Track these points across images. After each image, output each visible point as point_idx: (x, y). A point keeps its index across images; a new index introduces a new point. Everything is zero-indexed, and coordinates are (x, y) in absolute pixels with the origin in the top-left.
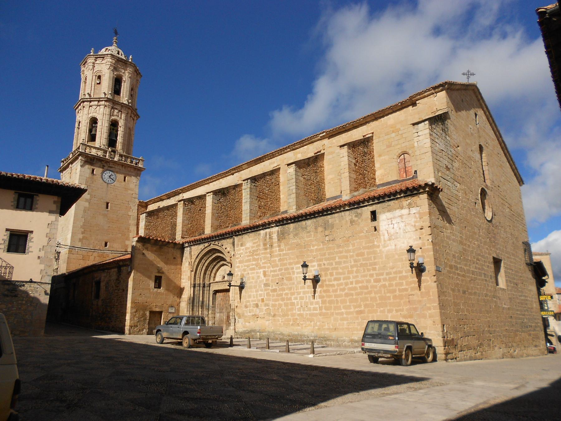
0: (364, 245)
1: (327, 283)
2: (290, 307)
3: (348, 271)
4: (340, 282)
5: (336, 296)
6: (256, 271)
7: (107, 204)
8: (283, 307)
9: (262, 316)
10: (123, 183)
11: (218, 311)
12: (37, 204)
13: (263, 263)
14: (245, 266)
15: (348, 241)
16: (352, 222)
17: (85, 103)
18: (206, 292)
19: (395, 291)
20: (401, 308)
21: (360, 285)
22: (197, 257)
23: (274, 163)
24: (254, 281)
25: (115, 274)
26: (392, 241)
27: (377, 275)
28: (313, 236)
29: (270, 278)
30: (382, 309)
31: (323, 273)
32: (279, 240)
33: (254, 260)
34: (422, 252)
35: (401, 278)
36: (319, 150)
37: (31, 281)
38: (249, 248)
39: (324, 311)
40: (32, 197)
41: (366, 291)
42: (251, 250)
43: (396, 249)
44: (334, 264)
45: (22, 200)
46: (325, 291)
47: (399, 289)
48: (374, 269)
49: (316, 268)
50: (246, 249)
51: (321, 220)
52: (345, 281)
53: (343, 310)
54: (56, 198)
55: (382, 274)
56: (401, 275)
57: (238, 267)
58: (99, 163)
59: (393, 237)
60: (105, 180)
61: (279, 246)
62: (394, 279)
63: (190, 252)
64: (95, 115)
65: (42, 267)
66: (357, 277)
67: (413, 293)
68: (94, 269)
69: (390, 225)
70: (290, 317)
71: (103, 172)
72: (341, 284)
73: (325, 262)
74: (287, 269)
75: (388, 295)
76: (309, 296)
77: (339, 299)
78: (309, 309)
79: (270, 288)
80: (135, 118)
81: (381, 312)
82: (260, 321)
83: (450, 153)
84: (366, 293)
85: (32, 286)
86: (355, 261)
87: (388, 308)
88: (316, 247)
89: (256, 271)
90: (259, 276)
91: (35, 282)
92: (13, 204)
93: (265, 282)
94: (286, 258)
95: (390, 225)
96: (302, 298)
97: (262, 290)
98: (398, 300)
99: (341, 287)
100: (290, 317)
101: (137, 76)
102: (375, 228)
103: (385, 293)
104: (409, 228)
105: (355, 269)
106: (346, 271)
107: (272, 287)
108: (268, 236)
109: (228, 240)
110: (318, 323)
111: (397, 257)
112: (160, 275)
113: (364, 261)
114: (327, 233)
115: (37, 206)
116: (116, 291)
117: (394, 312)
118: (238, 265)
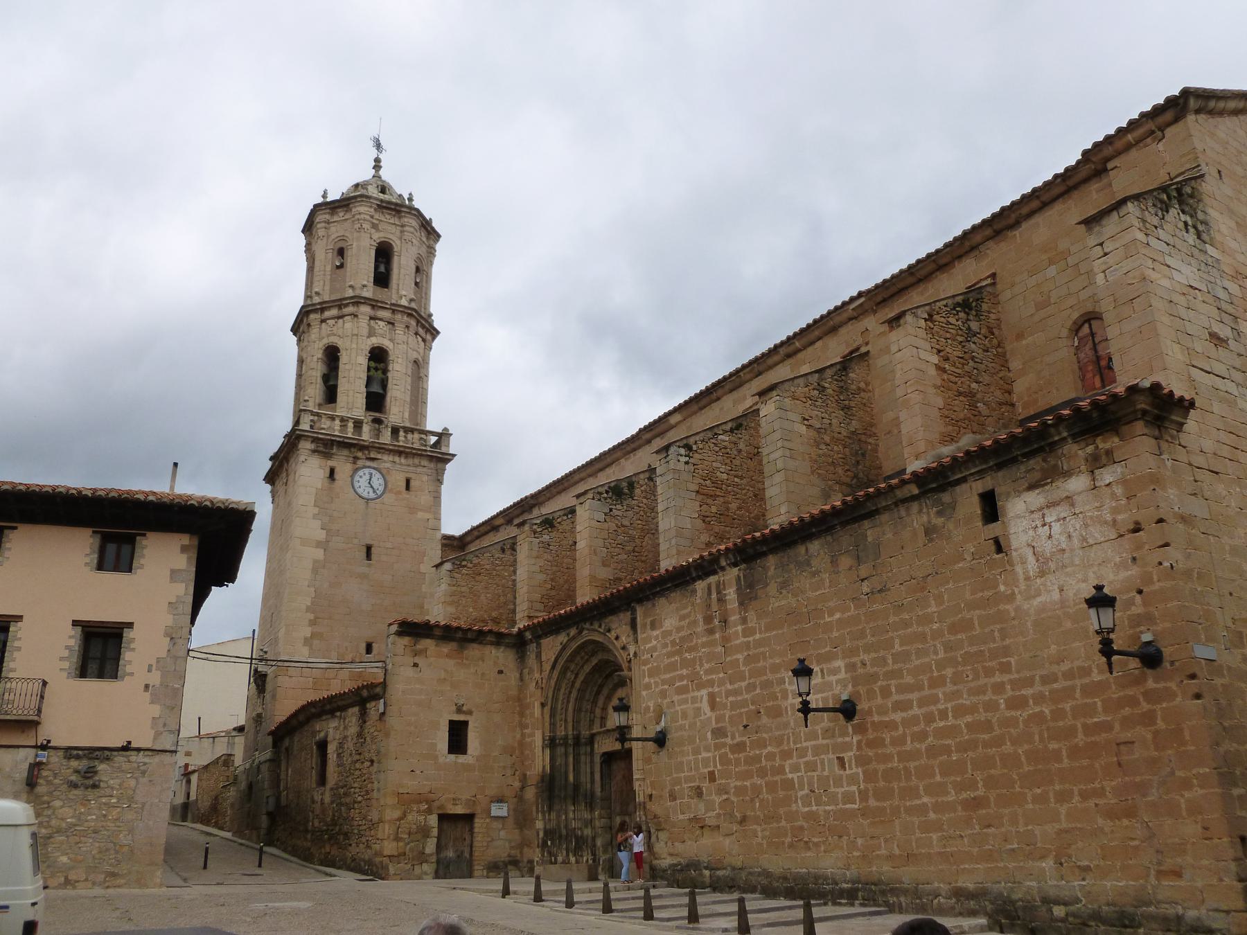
0: (968, 596)
1: (876, 718)
2: (781, 794)
3: (931, 678)
4: (911, 713)
5: (904, 757)
6: (689, 696)
7: (369, 549)
8: (765, 795)
9: (713, 822)
10: (405, 495)
11: (618, 810)
12: (143, 556)
13: (707, 672)
14: (664, 682)
15: (923, 589)
16: (929, 531)
17: (312, 316)
18: (583, 758)
19: (1070, 732)
20: (1097, 785)
21: (969, 719)
22: (553, 667)
23: (745, 398)
24: (687, 723)
25: (354, 720)
26: (1051, 577)
27: (1015, 684)
28: (827, 584)
29: (728, 714)
30: (1039, 791)
31: (862, 690)
32: (741, 604)
33: (685, 663)
34: (1145, 604)
35: (1088, 691)
36: (855, 346)
37: (126, 748)
38: (669, 633)
39: (872, 803)
40: (131, 541)
41: (986, 736)
42: (676, 637)
43: (1063, 603)
44: (890, 661)
45: (111, 548)
46: (871, 744)
47: (1085, 726)
48: (1005, 668)
49: (842, 675)
50: (667, 634)
51: (845, 538)
52: (923, 710)
53: (925, 800)
54: (185, 539)
55: (1030, 682)
56: (1086, 680)
57: (648, 686)
58: (345, 452)
59: (1052, 565)
60: (360, 491)
61: (744, 621)
62: (1068, 693)
63: (539, 655)
64: (334, 340)
65: (156, 710)
66: (956, 695)
67: (1128, 735)
68: (313, 710)
69: (1040, 530)
70: (783, 823)
71: (356, 470)
72: (914, 720)
73: (866, 657)
74: (767, 685)
75: (1053, 746)
76: (829, 760)
77: (912, 765)
78: (833, 799)
79: (729, 740)
80: (429, 337)
81: (1036, 799)
82: (707, 841)
83: (1222, 294)
84: (986, 745)
85: (133, 758)
86: (948, 647)
87: (1057, 787)
88: (837, 616)
89: (692, 694)
90: (699, 709)
91: (138, 750)
92: (87, 560)
93: (714, 725)
94: (763, 654)
95: (1040, 530)
96: (811, 767)
97: (707, 749)
98: (1085, 762)
99: (916, 729)
100: (783, 823)
101: (428, 238)
102: (997, 542)
103: (1042, 740)
104: (1097, 533)
105: (949, 672)
106: (925, 679)
107: (733, 738)
108: (714, 596)
109: (622, 615)
110: (860, 841)
111: (1068, 624)
112: (461, 718)
113: (971, 645)
114: (864, 571)
115: (142, 561)
116: (358, 765)
117: (1076, 798)
118: (647, 680)
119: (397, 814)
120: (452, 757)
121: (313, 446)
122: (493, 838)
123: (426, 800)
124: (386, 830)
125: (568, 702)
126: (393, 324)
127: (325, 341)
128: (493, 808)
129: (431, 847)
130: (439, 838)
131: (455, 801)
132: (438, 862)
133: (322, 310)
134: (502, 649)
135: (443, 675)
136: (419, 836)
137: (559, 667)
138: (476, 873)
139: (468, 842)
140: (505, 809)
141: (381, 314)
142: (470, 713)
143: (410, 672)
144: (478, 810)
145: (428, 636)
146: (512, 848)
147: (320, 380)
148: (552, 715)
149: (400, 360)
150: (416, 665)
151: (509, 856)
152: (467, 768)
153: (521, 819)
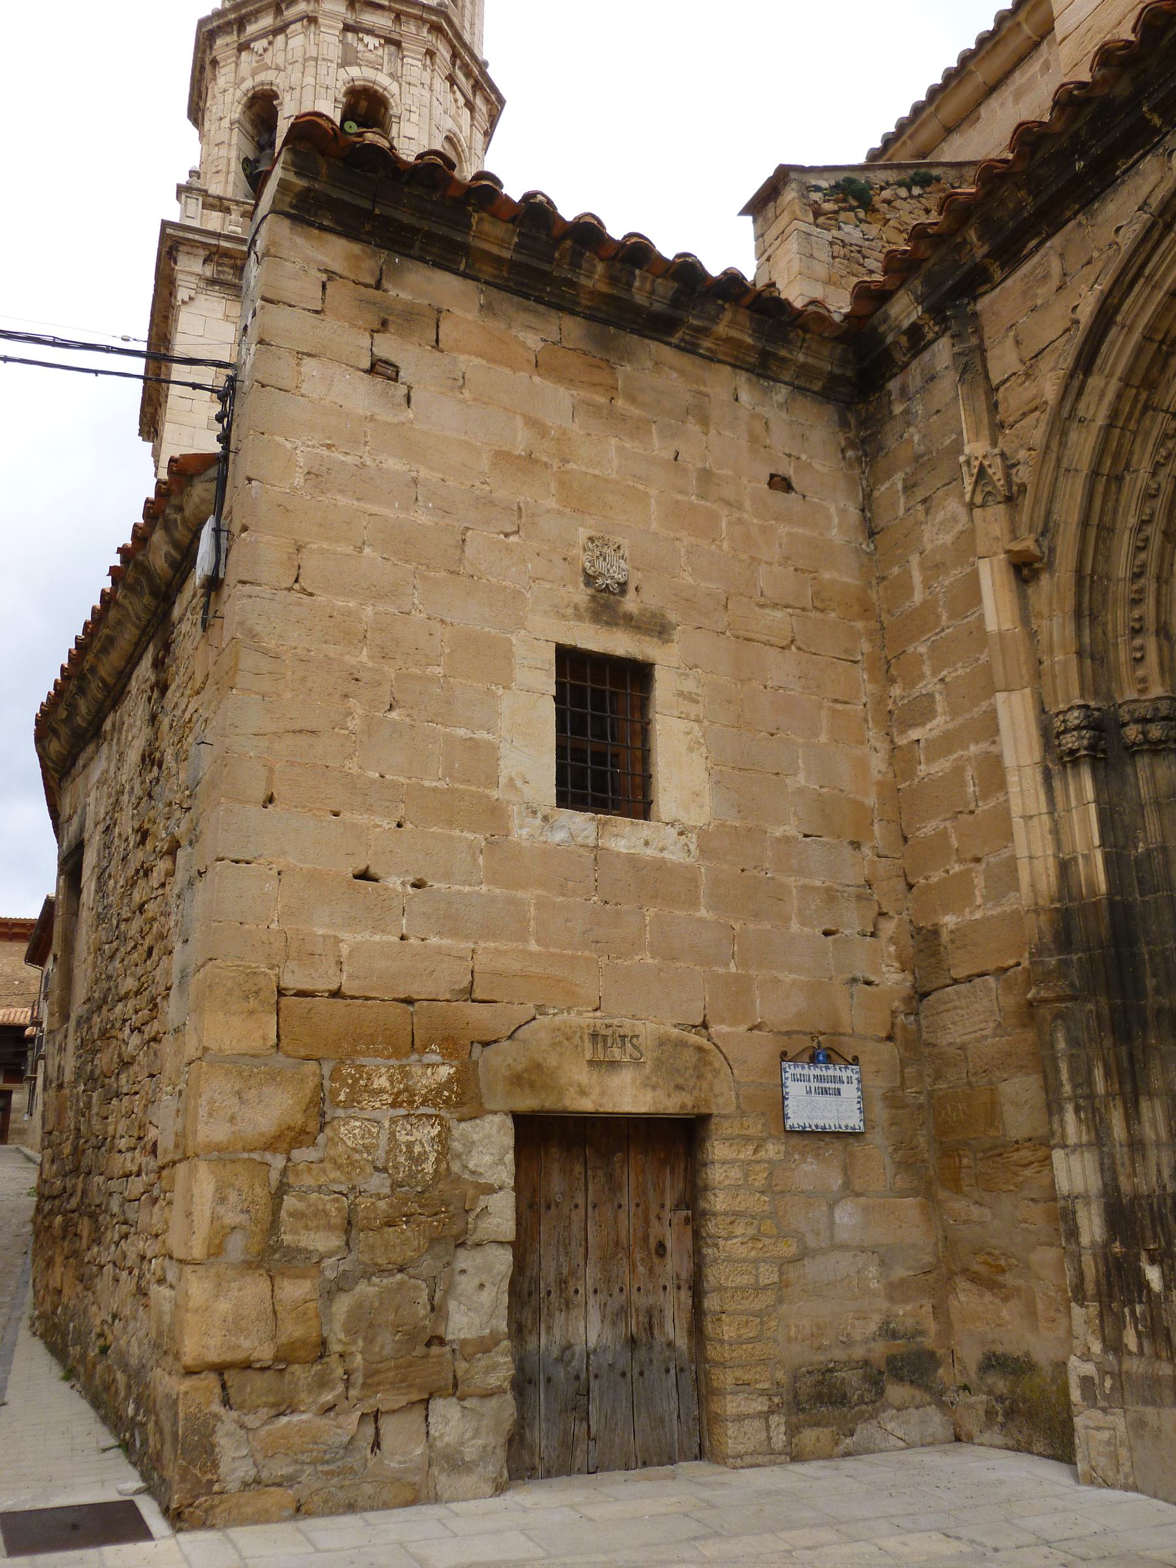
17: (220, 42)
22: (1086, 360)
119: (274, 1108)
120: (579, 824)
121: (208, 271)
122: (806, 1237)
123: (445, 1034)
124: (201, 1202)
126: (398, 44)
127: (248, 84)
128: (795, 1090)
129: (476, 1304)
130: (523, 1246)
131: (605, 1047)
132: (523, 1384)
133: (241, 23)
134: (781, 393)
135: (520, 439)
136: (406, 1240)
137: (1120, 351)
138: (736, 1438)
139: (676, 1264)
140: (850, 1091)
141: (370, 18)
142: (660, 629)
143: (360, 396)
144: (722, 1098)
145: (449, 255)
146: (896, 1291)
147: (235, 167)
148: (1087, 610)
149: (414, 117)
150: (381, 369)
151: (889, 1332)
152: (653, 880)
153: (943, 1141)
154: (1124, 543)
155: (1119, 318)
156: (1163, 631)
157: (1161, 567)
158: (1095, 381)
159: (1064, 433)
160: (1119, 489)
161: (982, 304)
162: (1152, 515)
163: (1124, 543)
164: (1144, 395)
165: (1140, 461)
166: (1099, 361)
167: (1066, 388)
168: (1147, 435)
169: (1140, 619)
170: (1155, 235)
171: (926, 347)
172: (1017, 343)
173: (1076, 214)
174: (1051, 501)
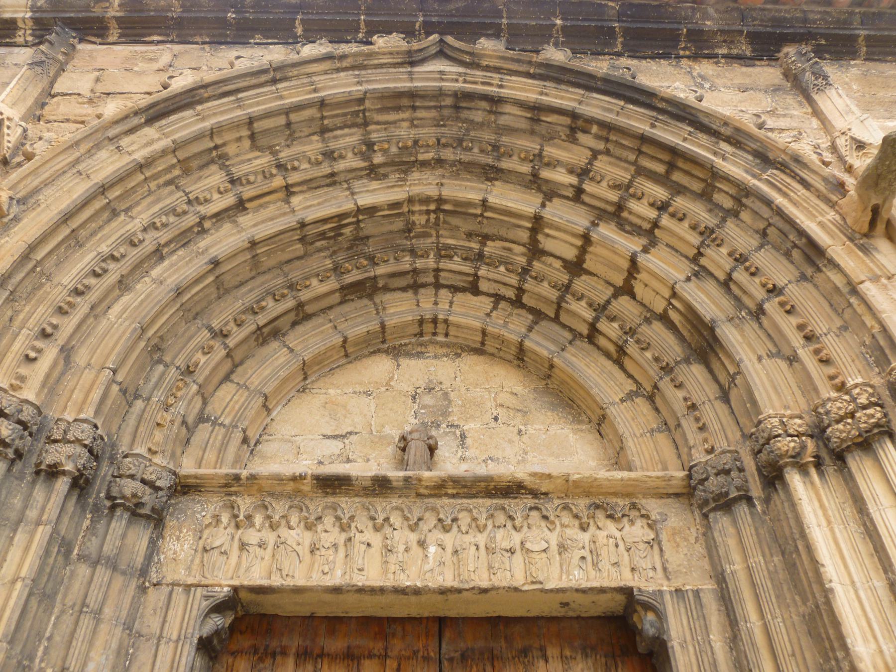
125: (123, 285)
137: (184, 125)
154: (85, 260)
155: (199, 108)
156: (67, 352)
157: (101, 301)
158: (150, 132)
159: (98, 146)
160: (109, 221)
161: (83, 47)
162: (123, 256)
163: (85, 260)
164: (177, 172)
165: (140, 213)
166: (164, 122)
167: (127, 117)
168: (158, 200)
169: (55, 327)
170: (263, 78)
171: (7, 45)
172: (98, 80)
173: (203, 43)
174: (46, 184)
